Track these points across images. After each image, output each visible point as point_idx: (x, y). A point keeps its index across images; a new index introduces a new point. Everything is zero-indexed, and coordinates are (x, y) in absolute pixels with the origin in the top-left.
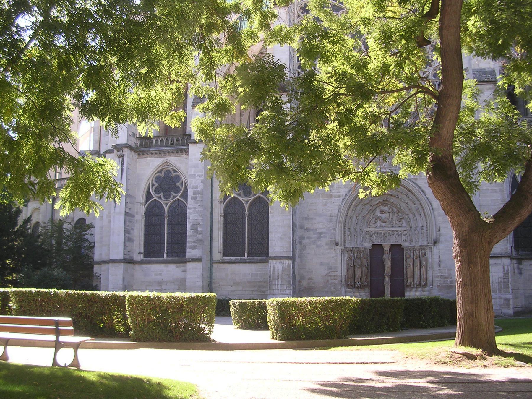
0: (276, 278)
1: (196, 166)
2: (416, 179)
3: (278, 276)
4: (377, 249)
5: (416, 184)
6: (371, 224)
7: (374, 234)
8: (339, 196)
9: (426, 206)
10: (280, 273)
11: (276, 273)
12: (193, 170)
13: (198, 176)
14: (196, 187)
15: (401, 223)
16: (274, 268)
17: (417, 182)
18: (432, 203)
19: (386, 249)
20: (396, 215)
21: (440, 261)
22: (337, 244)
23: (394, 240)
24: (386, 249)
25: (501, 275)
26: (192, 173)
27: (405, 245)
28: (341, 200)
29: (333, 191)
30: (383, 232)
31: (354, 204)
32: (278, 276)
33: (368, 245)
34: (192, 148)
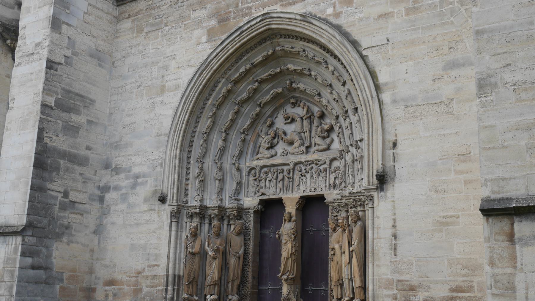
5: (338, 28)
6: (261, 150)
7: (266, 173)
8: (177, 88)
15: (328, 140)
17: (342, 21)
18: (377, 70)
19: (291, 208)
20: (316, 122)
21: (395, 236)
23: (307, 187)
24: (291, 208)
27: (331, 195)
28: (180, 96)
29: (166, 78)
30: (285, 168)
31: (210, 102)
33: (250, 202)
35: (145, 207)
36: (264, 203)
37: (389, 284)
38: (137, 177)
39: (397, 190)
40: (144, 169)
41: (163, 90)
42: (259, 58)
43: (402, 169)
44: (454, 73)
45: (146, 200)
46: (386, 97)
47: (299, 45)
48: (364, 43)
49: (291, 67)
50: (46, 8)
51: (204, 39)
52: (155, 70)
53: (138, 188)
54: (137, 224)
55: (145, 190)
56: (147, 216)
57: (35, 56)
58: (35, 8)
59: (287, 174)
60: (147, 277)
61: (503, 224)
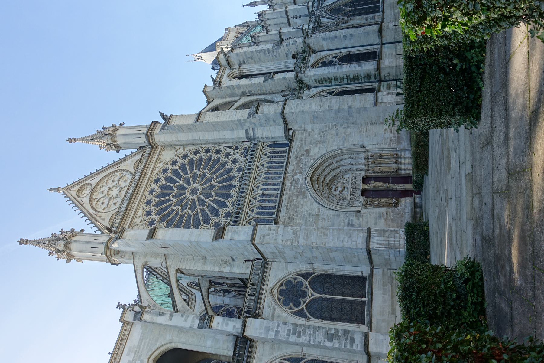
0: (387, 242)
1: (268, 329)
2: (314, 159)
3: (386, 241)
4: (364, 192)
8: (319, 209)
9: (336, 153)
10: (382, 238)
11: (382, 242)
12: (270, 333)
13: (278, 328)
14: (289, 330)
16: (378, 244)
17: (316, 158)
22: (359, 211)
23: (359, 182)
25: (390, 96)
26: (274, 333)
32: (386, 241)
33: (362, 198)
34: (249, 333)
35: (361, 219)
36: (362, 195)
37: (390, 145)
38: (349, 224)
39: (366, 144)
40: (346, 221)
41: (318, 215)
42: (317, 186)
43: (361, 143)
44: (339, 134)
45: (359, 219)
46: (341, 147)
47: (317, 174)
48: (325, 152)
49: (322, 180)
50: (279, 229)
51: (305, 199)
52: (309, 219)
53: (354, 223)
54: (367, 223)
55: (355, 221)
56: (365, 219)
57: (298, 233)
58: (277, 236)
59: (355, 187)
60: (387, 217)
61: (378, 104)
